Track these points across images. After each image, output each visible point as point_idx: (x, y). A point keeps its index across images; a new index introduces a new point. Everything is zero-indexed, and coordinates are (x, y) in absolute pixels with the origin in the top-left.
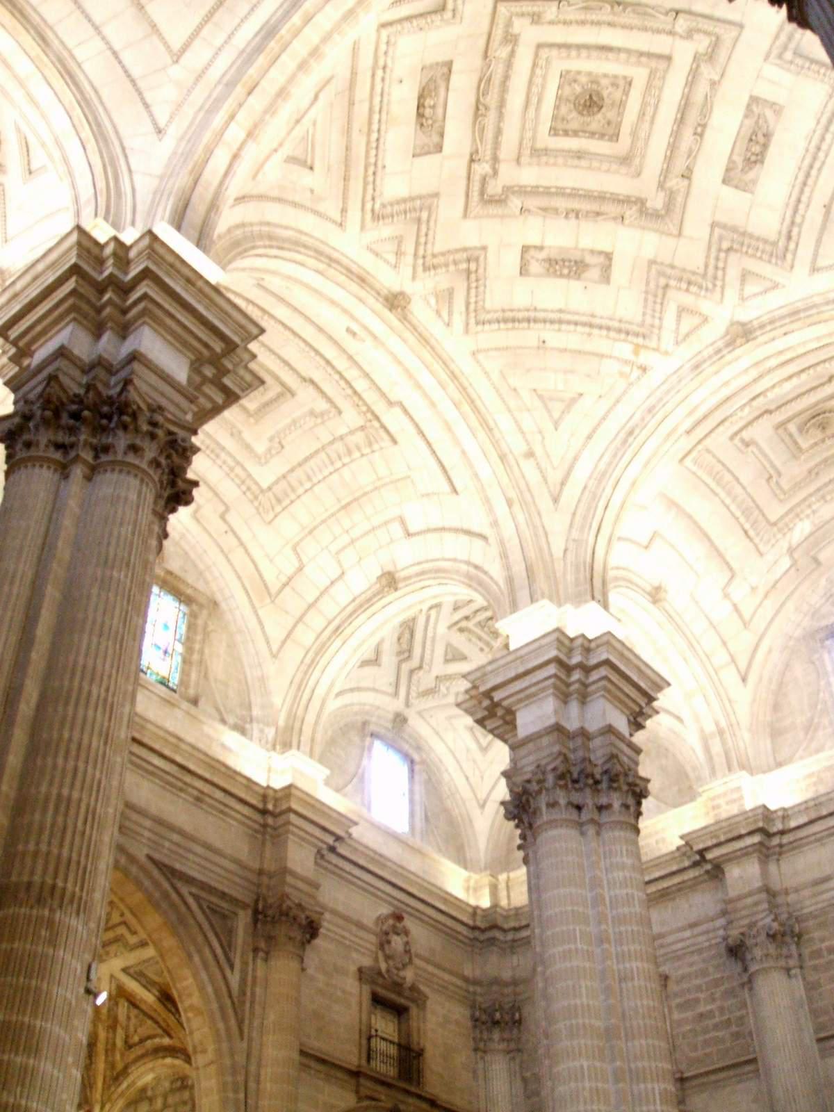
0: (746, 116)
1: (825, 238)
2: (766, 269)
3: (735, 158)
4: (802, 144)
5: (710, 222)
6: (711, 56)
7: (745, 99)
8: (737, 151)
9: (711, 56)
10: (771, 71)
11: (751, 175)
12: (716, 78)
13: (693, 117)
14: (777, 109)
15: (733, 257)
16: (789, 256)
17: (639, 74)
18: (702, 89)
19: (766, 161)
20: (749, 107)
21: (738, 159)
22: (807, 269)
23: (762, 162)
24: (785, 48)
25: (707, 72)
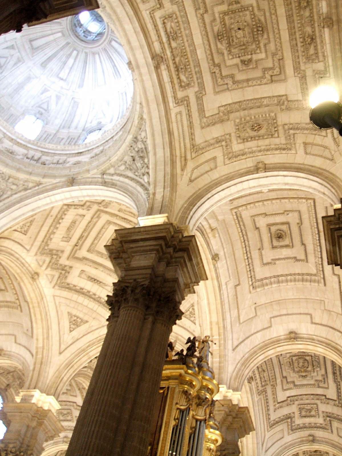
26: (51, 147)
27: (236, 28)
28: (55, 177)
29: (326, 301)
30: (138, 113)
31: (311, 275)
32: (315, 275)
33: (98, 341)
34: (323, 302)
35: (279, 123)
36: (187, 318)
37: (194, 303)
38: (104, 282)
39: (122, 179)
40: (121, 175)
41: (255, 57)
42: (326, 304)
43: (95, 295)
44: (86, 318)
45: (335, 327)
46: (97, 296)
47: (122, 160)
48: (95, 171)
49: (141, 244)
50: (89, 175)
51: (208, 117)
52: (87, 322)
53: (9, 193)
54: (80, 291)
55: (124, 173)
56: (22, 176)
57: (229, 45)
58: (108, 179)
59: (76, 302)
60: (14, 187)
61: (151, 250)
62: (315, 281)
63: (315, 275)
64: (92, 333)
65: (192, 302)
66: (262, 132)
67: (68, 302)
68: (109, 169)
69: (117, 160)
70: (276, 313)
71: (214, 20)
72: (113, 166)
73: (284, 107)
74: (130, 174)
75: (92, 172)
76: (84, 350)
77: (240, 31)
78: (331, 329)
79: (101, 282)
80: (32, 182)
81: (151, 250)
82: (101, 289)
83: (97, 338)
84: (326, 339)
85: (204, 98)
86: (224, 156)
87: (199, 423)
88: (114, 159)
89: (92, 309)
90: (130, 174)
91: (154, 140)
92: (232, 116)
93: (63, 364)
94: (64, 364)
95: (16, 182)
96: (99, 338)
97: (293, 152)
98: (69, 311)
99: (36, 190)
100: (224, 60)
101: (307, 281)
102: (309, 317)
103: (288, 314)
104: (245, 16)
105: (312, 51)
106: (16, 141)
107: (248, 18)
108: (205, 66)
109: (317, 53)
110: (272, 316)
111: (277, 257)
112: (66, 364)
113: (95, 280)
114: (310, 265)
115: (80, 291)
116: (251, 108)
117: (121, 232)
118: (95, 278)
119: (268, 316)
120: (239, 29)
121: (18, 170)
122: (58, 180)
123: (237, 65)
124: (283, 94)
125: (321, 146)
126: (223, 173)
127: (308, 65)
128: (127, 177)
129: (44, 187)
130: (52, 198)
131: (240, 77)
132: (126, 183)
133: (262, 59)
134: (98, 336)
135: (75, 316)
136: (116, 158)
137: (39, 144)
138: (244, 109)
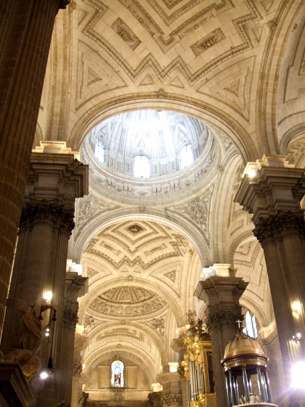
0: (135, 35)
1: (87, 47)
2: (85, 22)
3: (124, 25)
4: (119, 51)
5: (109, 7)
6: (161, 38)
7: (141, 39)
8: (126, 27)
9: (161, 38)
10: (146, 53)
11: (116, 27)
12: (154, 36)
13: (146, 21)
14: (134, 48)
15: (94, 11)
16: (88, 34)
17: (169, 12)
18: (153, 30)
19: (118, 35)
20: (137, 38)
21: (122, 26)
22: (80, 39)
23: (118, 33)
24: (153, 63)
25: (157, 35)
26: (121, 176)
28: (130, 203)
29: (251, 277)
30: (207, 187)
31: (247, 262)
32: (249, 263)
33: (104, 285)
34: (249, 277)
36: (168, 277)
37: (176, 270)
38: (114, 248)
39: (181, 218)
40: (180, 215)
43: (106, 256)
44: (97, 270)
45: (254, 291)
46: (107, 257)
48: (160, 206)
49: (225, 286)
50: (155, 208)
52: (98, 272)
54: (99, 254)
55: (183, 214)
56: (109, 201)
58: (170, 214)
59: (93, 260)
60: (102, 207)
62: (248, 266)
64: (100, 280)
65: (174, 269)
67: (88, 260)
72: (174, 206)
74: (187, 216)
76: (95, 291)
78: (251, 293)
79: (112, 248)
82: (111, 252)
83: (103, 283)
84: (247, 297)
86: (248, 220)
88: (177, 203)
89: (102, 265)
90: (187, 216)
91: (219, 210)
93: (83, 301)
94: (84, 302)
95: (103, 203)
96: (104, 283)
98: (89, 266)
99: (117, 211)
101: (244, 265)
106: (100, 170)
112: (85, 302)
113: (109, 247)
114: (248, 257)
115: (99, 254)
118: (109, 245)
121: (107, 196)
122: (132, 206)
126: (245, 230)
128: (186, 218)
129: (122, 209)
132: (185, 223)
134: (104, 282)
135: (91, 269)
137: (113, 172)
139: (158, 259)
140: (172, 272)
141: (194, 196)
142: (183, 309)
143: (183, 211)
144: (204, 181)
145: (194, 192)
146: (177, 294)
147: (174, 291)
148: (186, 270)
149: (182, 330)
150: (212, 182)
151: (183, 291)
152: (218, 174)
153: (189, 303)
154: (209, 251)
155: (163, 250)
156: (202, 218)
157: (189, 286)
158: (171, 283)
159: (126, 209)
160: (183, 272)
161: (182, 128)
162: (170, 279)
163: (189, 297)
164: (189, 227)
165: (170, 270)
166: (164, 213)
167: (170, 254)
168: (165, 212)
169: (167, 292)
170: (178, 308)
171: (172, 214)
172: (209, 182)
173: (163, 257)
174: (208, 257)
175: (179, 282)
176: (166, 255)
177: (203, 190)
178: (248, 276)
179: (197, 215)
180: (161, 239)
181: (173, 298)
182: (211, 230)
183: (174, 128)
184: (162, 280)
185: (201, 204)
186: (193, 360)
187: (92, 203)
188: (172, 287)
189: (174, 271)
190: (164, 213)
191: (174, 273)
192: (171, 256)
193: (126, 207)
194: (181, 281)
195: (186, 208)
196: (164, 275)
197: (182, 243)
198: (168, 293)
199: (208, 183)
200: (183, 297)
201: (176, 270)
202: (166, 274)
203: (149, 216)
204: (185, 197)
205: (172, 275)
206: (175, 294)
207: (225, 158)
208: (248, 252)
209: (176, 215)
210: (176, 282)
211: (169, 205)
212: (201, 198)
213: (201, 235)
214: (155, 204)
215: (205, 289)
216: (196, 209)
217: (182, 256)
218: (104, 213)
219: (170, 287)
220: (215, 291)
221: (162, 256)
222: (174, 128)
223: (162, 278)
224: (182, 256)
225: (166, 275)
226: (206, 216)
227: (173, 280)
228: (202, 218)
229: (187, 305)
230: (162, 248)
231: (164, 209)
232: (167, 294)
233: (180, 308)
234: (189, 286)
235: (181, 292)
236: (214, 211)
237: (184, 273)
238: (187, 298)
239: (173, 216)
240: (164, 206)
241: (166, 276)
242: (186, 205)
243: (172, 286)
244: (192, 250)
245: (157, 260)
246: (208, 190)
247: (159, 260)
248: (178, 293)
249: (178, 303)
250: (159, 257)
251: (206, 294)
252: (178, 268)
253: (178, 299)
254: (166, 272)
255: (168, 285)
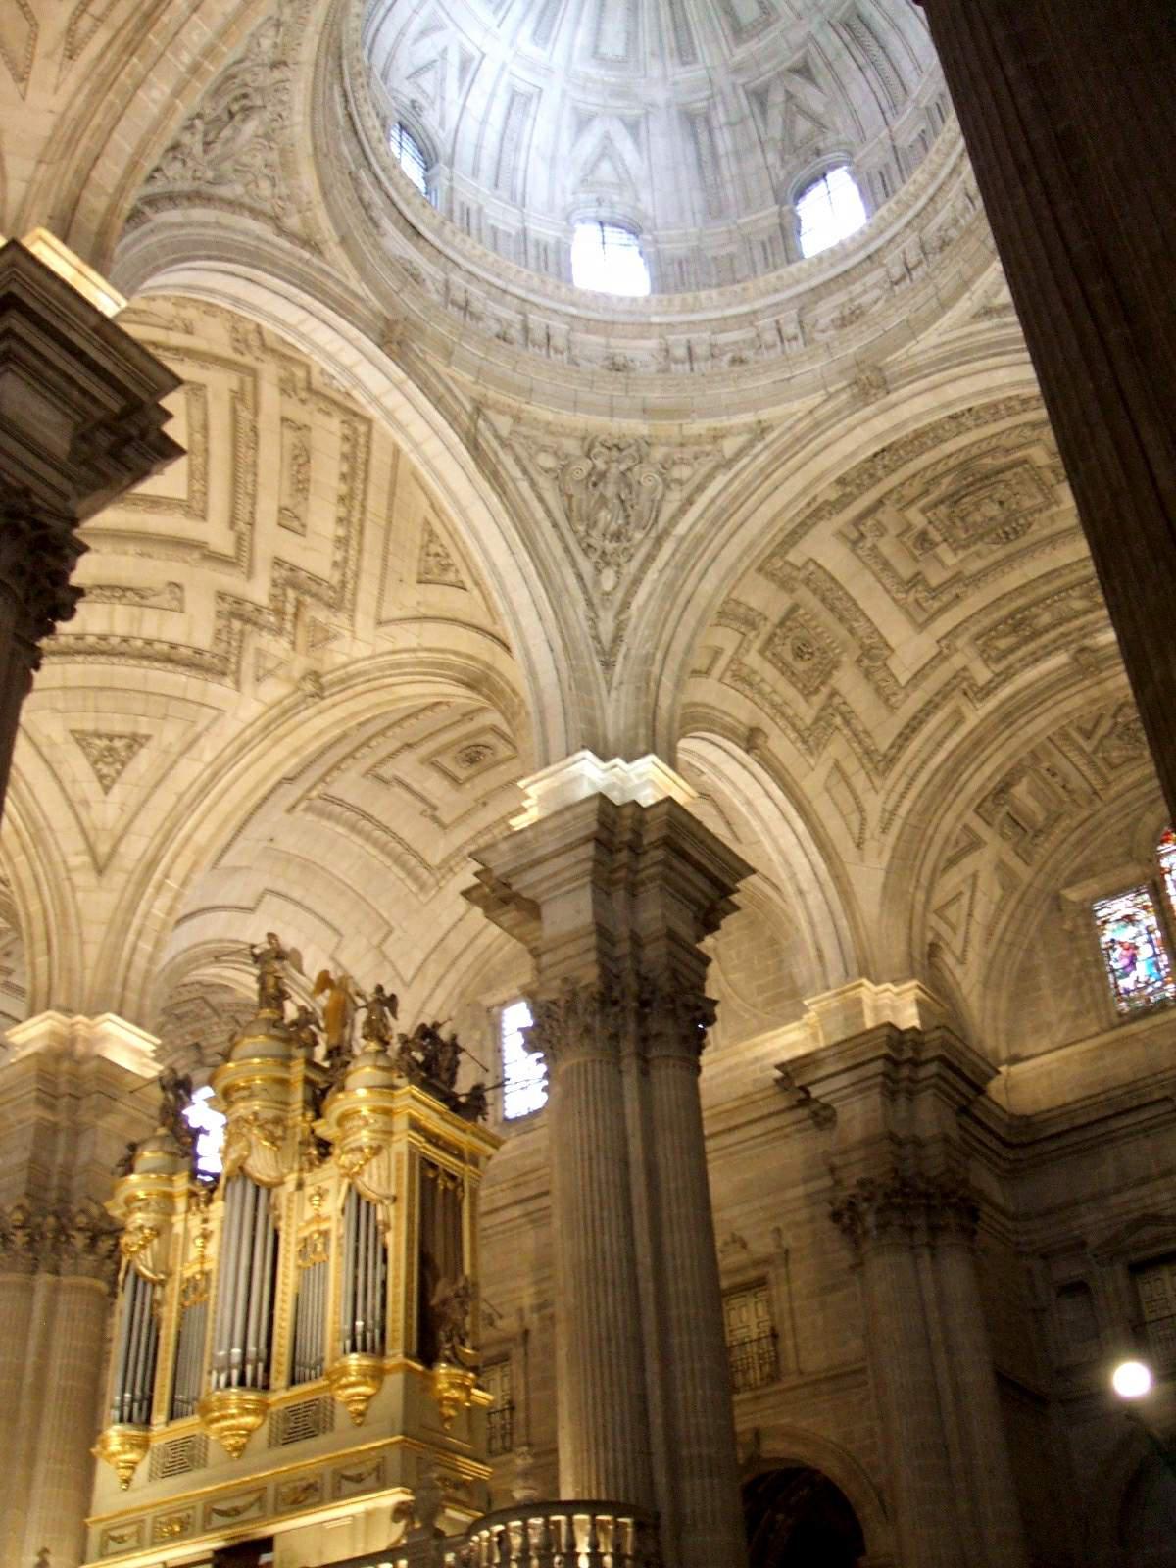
26: (370, 124)
27: (997, 496)
29: (397, 933)
31: (423, 861)
32: (428, 867)
34: (385, 929)
35: (832, 682)
36: (88, 755)
37: (148, 737)
39: (524, 486)
41: (941, 548)
42: (392, 938)
47: (552, 433)
48: (467, 378)
49: (688, 870)
50: (441, 367)
51: (787, 563)
53: (239, 190)
56: (307, 179)
57: (953, 499)
61: (692, 900)
62: (416, 879)
63: (428, 867)
65: (143, 730)
66: (800, 666)
68: (501, 412)
69: (548, 424)
70: (280, 886)
71: (1008, 451)
72: (517, 419)
73: (866, 662)
75: (455, 371)
77: (996, 506)
80: (304, 222)
81: (692, 900)
85: (822, 525)
87: (263, 1192)
88: (546, 414)
92: (804, 594)
97: (812, 761)
100: (912, 502)
102: (268, 897)
103: (298, 903)
104: (1032, 496)
105: (1003, 644)
107: (1027, 503)
108: (894, 479)
109: (1004, 654)
110: (270, 886)
111: (408, 780)
114: (442, 843)
116: (832, 609)
117: (677, 812)
119: (266, 882)
120: (1001, 503)
122: (362, 290)
123: (909, 527)
124: (892, 642)
125: (856, 798)
127: (971, 652)
129: (323, 271)
130: (314, 323)
131: (887, 547)
133: (941, 562)
136: (549, 416)
138: (824, 600)
139: (91, 640)
140: (121, 737)
141: (638, 427)
142: (95, 934)
143: (547, 461)
144: (724, 393)
145: (646, 412)
146: (91, 849)
147: (83, 832)
148: (208, 756)
149: (65, 1031)
150: (766, 414)
151: (134, 849)
152: (830, 397)
153: (147, 915)
154: (604, 692)
155: (148, 611)
156: (617, 536)
157: (188, 838)
158: (90, 787)
159: (338, 282)
160: (184, 761)
161: (625, 145)
162: (95, 763)
163: (159, 887)
164: (542, 545)
165: (119, 725)
166: (464, 418)
167: (173, 646)
168: (471, 417)
169: (42, 823)
170: (73, 921)
171: (495, 444)
172: (754, 405)
173: (124, 647)
174: (598, 714)
175: (133, 802)
176: (149, 642)
177: (698, 427)
178: (387, 923)
179: (604, 516)
180: (196, 555)
181: (65, 862)
182: (642, 608)
183: (583, 122)
184: (45, 750)
185: (647, 477)
186: (265, 1178)
187: (251, 127)
188: (80, 809)
189: (136, 741)
190: (464, 418)
191: (130, 747)
192: (170, 658)
193: (340, 271)
194: (146, 801)
195: (567, 456)
196: (72, 732)
197: (295, 626)
198: (49, 827)
199: (746, 410)
200: (117, 879)
201: (148, 737)
202: (82, 731)
203: (398, 386)
204: (591, 408)
205: (110, 749)
206: (81, 845)
207: (935, 347)
208: (461, 820)
209: (507, 460)
210: (116, 789)
211: (505, 398)
212: (658, 453)
213: (582, 606)
214: (448, 354)
215: (598, 841)
216: (610, 491)
217: (238, 684)
218: (255, 218)
219: (71, 806)
220: (637, 872)
221: (125, 640)
222: (583, 122)
223: (53, 744)
224: (238, 684)
225: (81, 738)
226: (641, 542)
227: (101, 777)
228: (617, 536)
229: (136, 922)
230: (153, 600)
231: (473, 400)
232: (39, 830)
233: (79, 926)
234: (188, 838)
235: (122, 848)
236: (699, 539)
237: (189, 772)
238: (150, 890)
239: (496, 454)
240: (477, 390)
241: (78, 741)
242: (572, 446)
243: (86, 803)
244: (324, 680)
245: (81, 645)
246: (717, 437)
247: (91, 651)
248: (103, 848)
249: (80, 895)
250: (103, 638)
251: (589, 865)
252: (170, 735)
253: (84, 879)
254: (89, 726)
255: (63, 789)
